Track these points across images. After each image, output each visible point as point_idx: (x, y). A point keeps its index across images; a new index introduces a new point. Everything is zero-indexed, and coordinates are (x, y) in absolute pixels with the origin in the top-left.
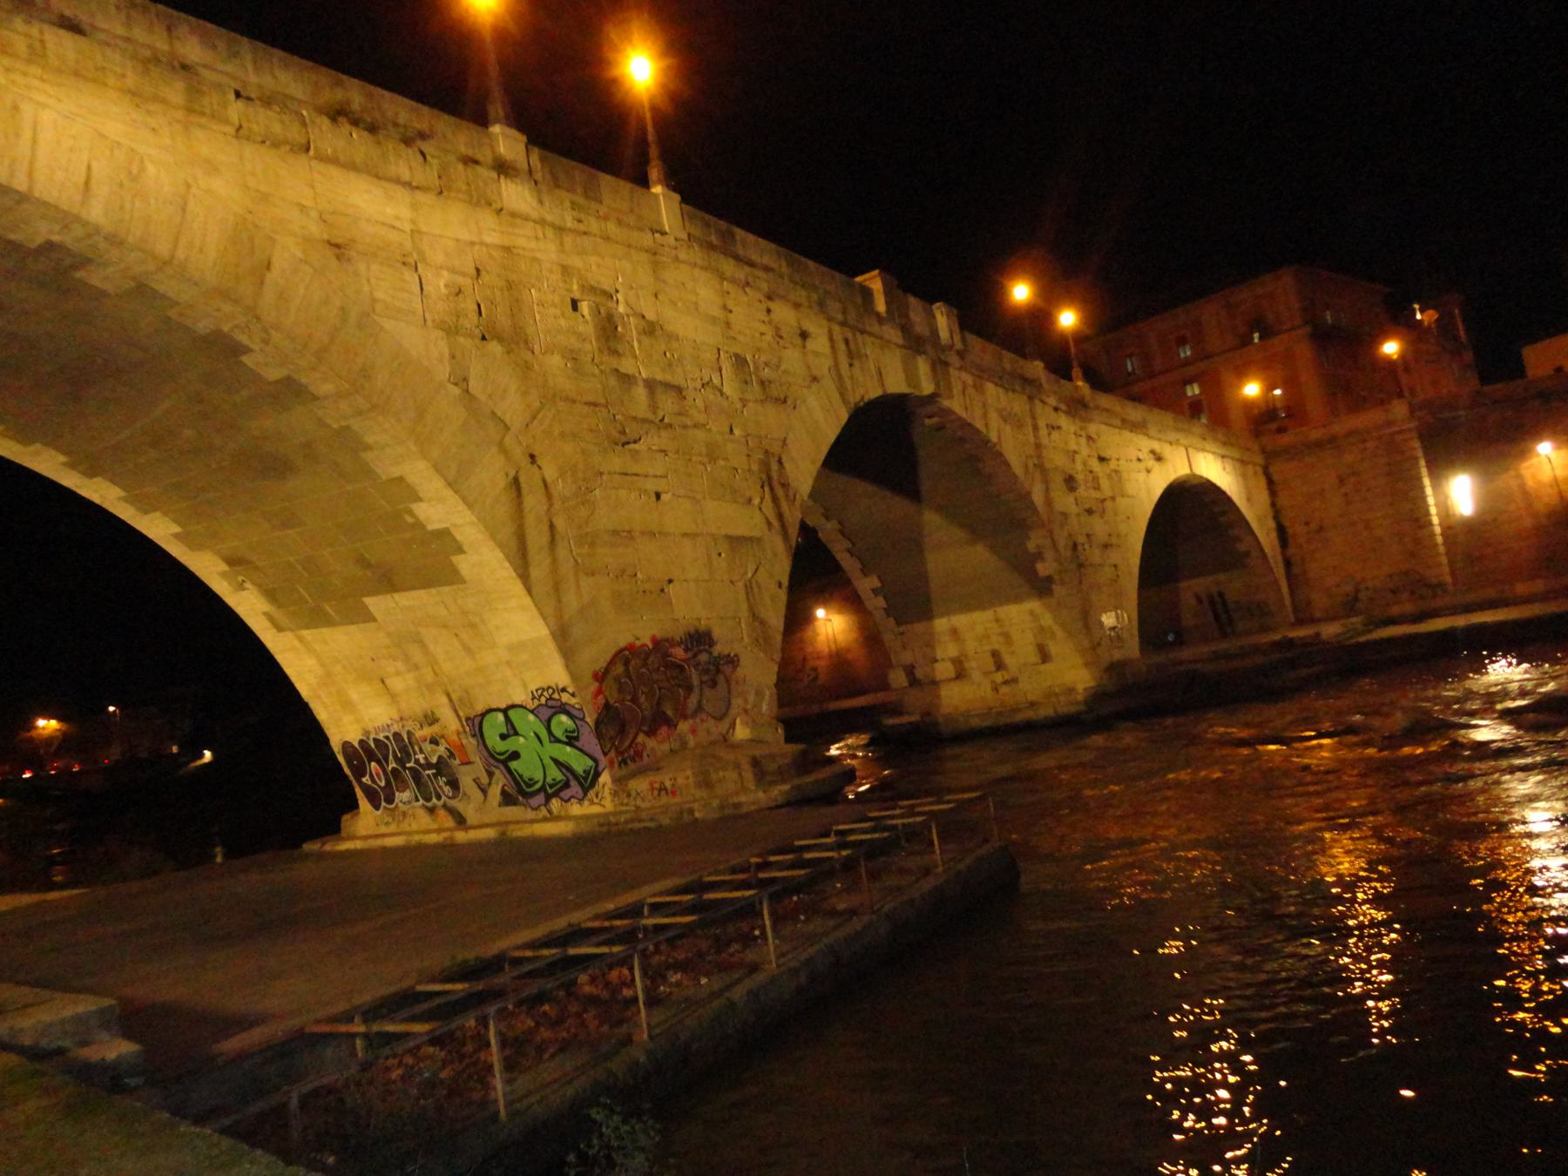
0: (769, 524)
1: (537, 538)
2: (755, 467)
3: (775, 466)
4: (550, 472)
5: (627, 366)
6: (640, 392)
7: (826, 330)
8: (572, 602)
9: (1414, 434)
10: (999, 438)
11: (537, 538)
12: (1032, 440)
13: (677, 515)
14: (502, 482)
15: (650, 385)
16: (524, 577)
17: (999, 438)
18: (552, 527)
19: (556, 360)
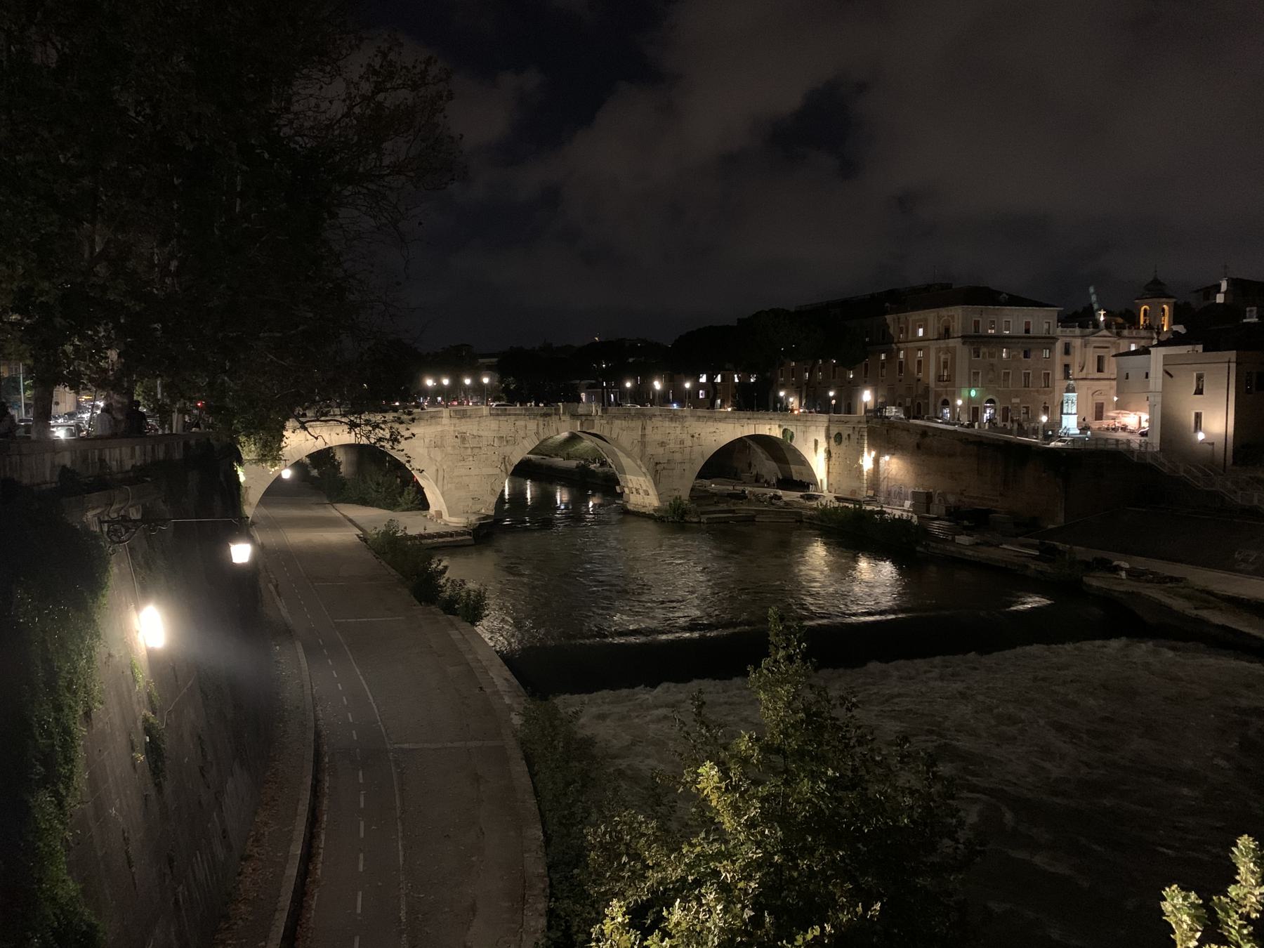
0: (502, 471)
1: (440, 478)
2: (500, 459)
3: (507, 458)
4: (445, 467)
5: (467, 446)
6: (469, 450)
7: (536, 424)
8: (446, 488)
9: (866, 430)
10: (618, 436)
11: (440, 478)
12: (640, 433)
13: (473, 472)
14: (434, 470)
15: (472, 448)
16: (437, 485)
17: (618, 436)
18: (444, 477)
19: (450, 448)
